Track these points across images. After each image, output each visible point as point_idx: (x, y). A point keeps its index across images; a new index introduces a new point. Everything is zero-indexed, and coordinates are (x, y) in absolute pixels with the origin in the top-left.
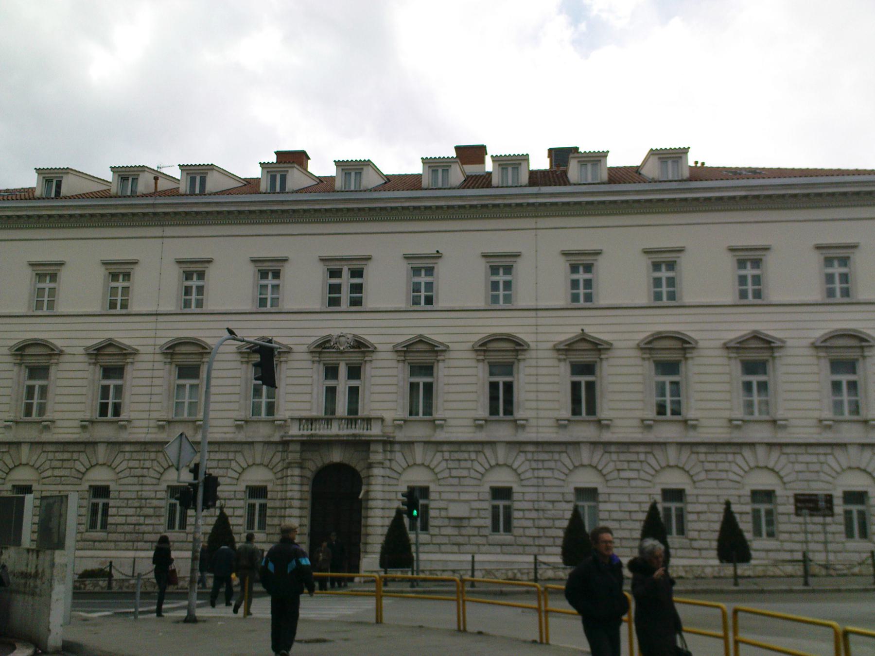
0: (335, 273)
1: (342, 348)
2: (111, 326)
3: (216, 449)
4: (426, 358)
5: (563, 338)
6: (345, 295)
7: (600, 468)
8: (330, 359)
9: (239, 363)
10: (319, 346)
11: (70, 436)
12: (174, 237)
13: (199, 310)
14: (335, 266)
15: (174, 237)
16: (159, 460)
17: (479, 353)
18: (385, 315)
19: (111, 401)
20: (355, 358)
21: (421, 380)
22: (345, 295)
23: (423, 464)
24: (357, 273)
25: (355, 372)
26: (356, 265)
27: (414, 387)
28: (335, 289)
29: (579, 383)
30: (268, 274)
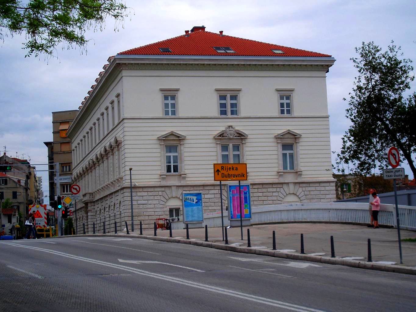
0: (223, 97)
1: (231, 137)
2: (155, 125)
3: (213, 189)
4: (289, 141)
5: (280, 132)
6: (229, 109)
7: (297, 194)
8: (225, 142)
9: (276, 143)
10: (220, 136)
11: (153, 183)
12: (182, 76)
13: (173, 117)
14: (223, 93)
15: (182, 76)
16: (281, 191)
17: (278, 139)
18: (184, 121)
19: (172, 164)
20: (237, 142)
21: (288, 152)
22: (229, 109)
23: (293, 193)
24: (234, 97)
25: (237, 148)
26: (234, 93)
27: (284, 155)
28: (223, 106)
29: (286, 154)
30: (168, 97)
